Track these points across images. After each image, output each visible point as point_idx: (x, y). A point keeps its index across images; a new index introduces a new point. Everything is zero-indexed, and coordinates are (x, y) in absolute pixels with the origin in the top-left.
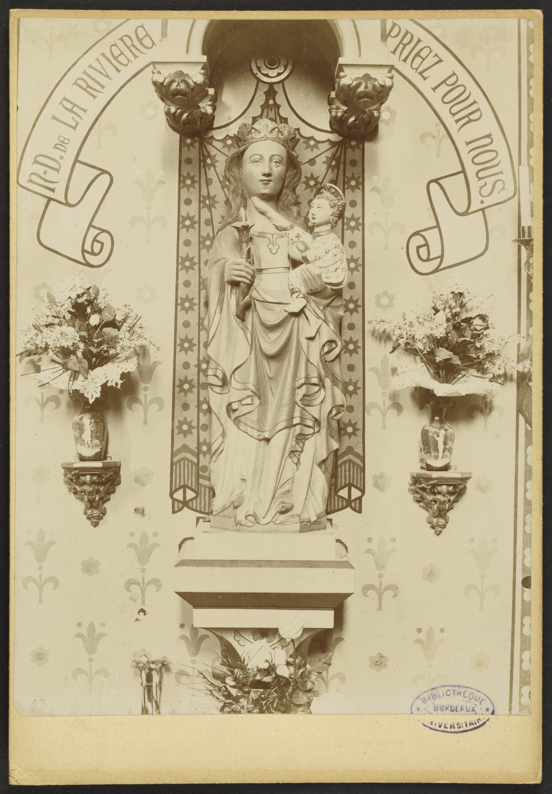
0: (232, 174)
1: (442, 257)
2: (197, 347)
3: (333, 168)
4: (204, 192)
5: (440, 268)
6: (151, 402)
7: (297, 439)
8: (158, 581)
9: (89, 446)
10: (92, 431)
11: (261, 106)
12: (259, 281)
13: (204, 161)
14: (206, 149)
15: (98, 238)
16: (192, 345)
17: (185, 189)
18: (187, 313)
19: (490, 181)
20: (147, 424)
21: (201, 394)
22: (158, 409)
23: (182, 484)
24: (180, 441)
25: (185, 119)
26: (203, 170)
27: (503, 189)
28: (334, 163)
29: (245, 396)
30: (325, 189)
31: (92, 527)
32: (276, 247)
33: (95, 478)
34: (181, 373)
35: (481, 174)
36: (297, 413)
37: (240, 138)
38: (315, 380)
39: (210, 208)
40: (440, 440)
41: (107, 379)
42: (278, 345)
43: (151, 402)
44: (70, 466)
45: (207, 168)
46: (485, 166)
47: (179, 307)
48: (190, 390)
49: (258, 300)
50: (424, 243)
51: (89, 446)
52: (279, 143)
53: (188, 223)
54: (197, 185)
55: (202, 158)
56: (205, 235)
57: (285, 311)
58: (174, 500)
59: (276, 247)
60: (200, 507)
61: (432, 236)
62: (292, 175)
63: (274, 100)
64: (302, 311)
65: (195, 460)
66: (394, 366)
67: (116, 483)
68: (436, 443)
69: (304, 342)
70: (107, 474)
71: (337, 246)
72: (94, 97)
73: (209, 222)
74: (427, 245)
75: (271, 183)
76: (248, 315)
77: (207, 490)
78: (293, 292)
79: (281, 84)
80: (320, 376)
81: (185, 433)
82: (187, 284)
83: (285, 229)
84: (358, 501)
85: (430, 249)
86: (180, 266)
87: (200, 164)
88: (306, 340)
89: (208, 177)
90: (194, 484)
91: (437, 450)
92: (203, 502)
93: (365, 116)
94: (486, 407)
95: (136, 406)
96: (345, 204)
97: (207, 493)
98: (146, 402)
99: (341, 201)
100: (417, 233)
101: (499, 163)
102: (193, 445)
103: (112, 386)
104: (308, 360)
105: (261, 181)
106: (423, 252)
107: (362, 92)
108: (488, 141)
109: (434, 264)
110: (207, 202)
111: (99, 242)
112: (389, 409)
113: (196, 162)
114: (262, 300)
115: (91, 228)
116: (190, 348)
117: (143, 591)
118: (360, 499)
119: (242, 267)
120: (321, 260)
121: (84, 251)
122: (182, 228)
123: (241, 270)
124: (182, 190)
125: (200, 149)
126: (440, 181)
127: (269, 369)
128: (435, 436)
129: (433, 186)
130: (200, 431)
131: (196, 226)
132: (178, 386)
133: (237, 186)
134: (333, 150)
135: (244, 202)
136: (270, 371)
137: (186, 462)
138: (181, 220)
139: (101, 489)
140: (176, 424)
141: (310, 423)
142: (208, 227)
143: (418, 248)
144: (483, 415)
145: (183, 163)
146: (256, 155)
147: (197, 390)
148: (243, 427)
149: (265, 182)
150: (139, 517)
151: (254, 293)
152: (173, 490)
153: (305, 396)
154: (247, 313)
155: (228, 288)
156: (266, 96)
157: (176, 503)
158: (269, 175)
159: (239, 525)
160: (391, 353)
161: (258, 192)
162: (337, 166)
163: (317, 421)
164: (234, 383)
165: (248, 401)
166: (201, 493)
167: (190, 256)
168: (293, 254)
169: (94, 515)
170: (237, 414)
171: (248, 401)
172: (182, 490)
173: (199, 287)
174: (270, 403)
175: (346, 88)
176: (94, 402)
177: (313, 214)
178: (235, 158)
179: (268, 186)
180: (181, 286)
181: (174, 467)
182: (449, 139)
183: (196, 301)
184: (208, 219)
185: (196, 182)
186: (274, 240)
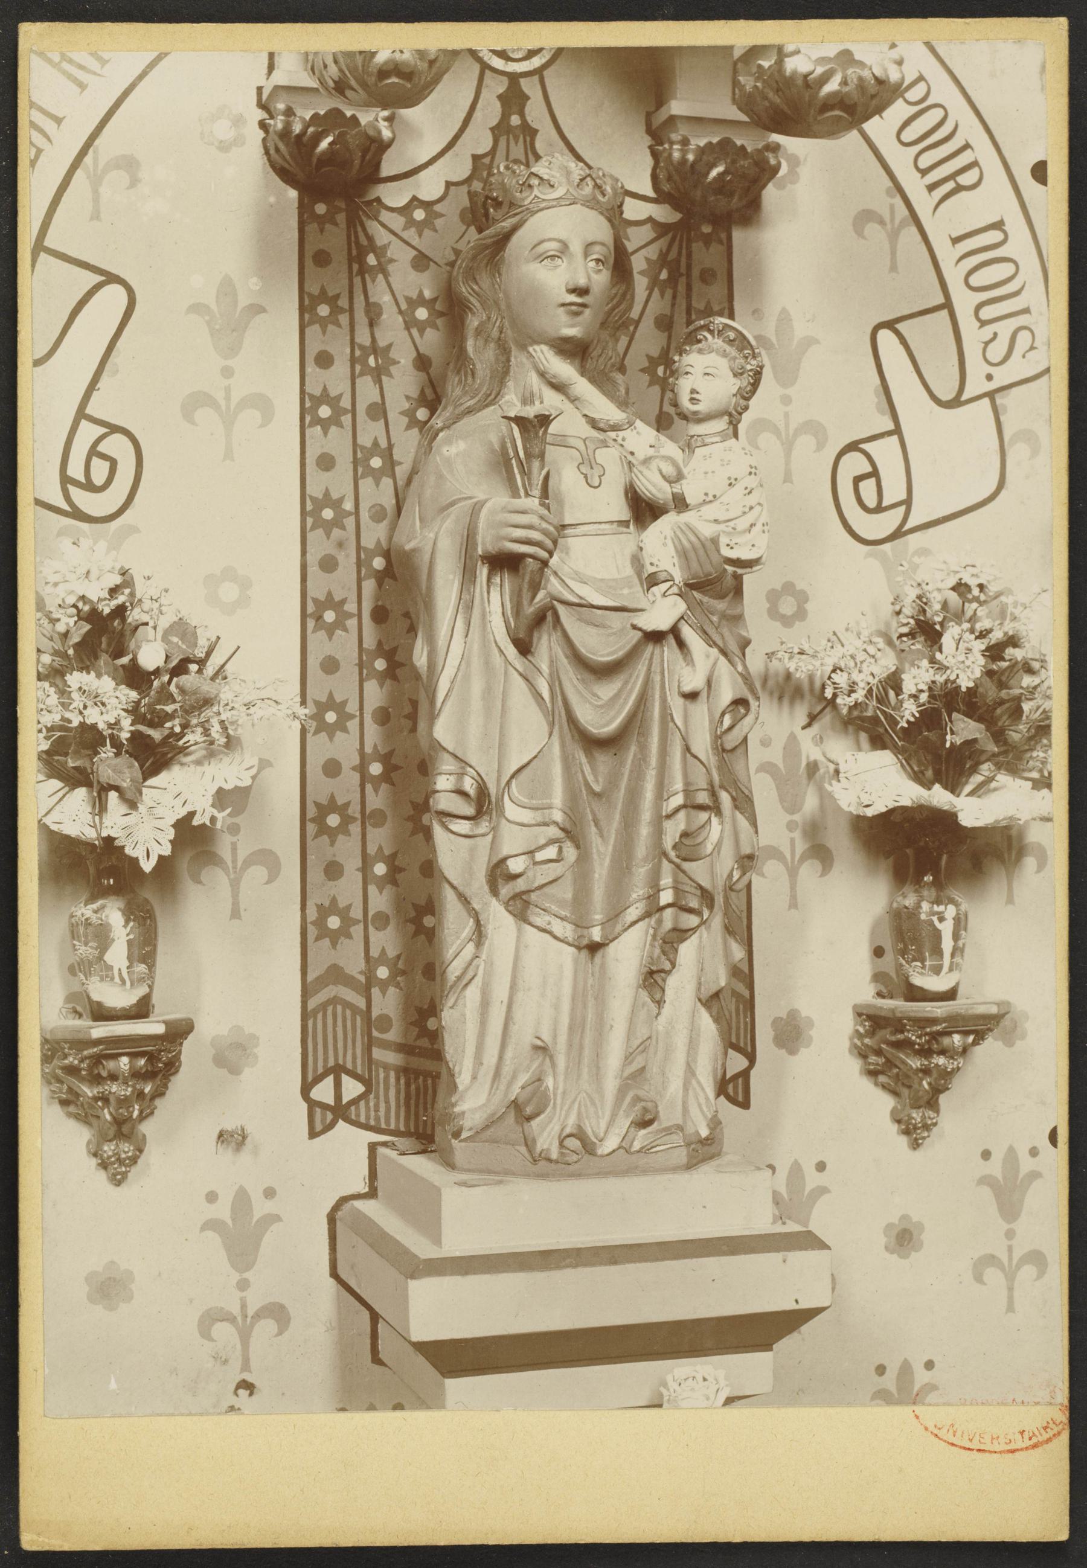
0: (475, 287)
1: (908, 502)
2: (357, 720)
3: (663, 286)
4: (363, 337)
5: (906, 528)
6: (248, 863)
7: (664, 942)
8: (282, 1307)
9: (123, 982)
10: (130, 943)
11: (492, 129)
12: (563, 555)
13: (360, 258)
14: (364, 229)
15: (101, 448)
16: (344, 717)
17: (316, 327)
18: (330, 635)
19: (1005, 329)
20: (240, 918)
21: (369, 837)
22: (266, 878)
23: (331, 1063)
24: (323, 955)
25: (324, 153)
26: (357, 280)
27: (1032, 348)
28: (664, 275)
29: (542, 841)
30: (711, 332)
31: (110, 1188)
32: (597, 471)
33: (142, 1062)
34: (321, 788)
35: (986, 313)
36: (666, 880)
37: (495, 199)
38: (703, 798)
39: (378, 375)
40: (946, 929)
41: (188, 808)
42: (619, 713)
43: (248, 863)
44: (81, 1036)
45: (367, 276)
46: (992, 295)
47: (311, 624)
48: (343, 828)
49: (563, 602)
50: (869, 469)
51: (123, 982)
52: (601, 213)
53: (325, 412)
54: (344, 319)
55: (354, 252)
56: (369, 444)
57: (634, 627)
58: (312, 1104)
59: (597, 471)
60: (377, 1119)
61: (886, 452)
62: (616, 294)
63: (522, 115)
64: (675, 631)
65: (361, 1003)
66: (812, 758)
67: (173, 1070)
68: (937, 935)
69: (677, 704)
70: (170, 1052)
71: (753, 470)
72: (82, 86)
73: (378, 411)
74: (875, 473)
75: (587, 312)
76: (539, 639)
77: (392, 1074)
78: (652, 581)
79: (536, 78)
80: (712, 786)
81: (334, 937)
82: (329, 564)
83: (615, 428)
84: (740, 1080)
85: (883, 484)
86: (310, 521)
87: (350, 268)
88: (681, 701)
89: (371, 300)
90: (359, 1062)
91: (938, 952)
92: (382, 1105)
93: (745, 163)
94: (1010, 847)
95: (207, 874)
96: (762, 367)
97: (392, 1080)
98: (234, 861)
99: (754, 362)
100: (853, 447)
101: (1023, 287)
102: (355, 966)
103: (204, 825)
104: (687, 749)
105: (563, 305)
106: (868, 488)
107: (835, 94)
108: (995, 236)
109: (889, 522)
110: (372, 361)
111: (104, 457)
112: (803, 859)
113: (339, 258)
114: (576, 600)
115: (84, 423)
116: (340, 726)
117: (245, 1337)
118: (745, 1074)
119: (534, 520)
120: (716, 504)
121: (66, 480)
122: (311, 425)
123: (530, 527)
124: (307, 330)
125: (348, 228)
126: (899, 326)
127: (595, 772)
128: (935, 919)
129: (884, 335)
130: (371, 928)
131: (347, 419)
132: (313, 820)
133: (489, 318)
134: (663, 243)
135: (504, 359)
136: (596, 777)
137: (339, 1008)
138: (308, 405)
139: (147, 1090)
140: (312, 914)
141: (694, 903)
142: (374, 424)
143: (858, 480)
144: (1003, 862)
145: (309, 262)
146: (550, 240)
147: (359, 829)
148: (540, 920)
149: (574, 308)
150: (227, 1154)
151: (554, 585)
152: (310, 1078)
153: (685, 835)
154: (536, 635)
155: (481, 573)
156: (503, 106)
157: (318, 1110)
158: (582, 292)
159: (543, 1163)
160: (804, 728)
161: (552, 333)
162: (673, 280)
163: (707, 897)
164: (511, 810)
165: (551, 852)
166: (378, 1083)
167: (335, 495)
168: (654, 491)
169: (123, 1156)
170: (520, 885)
171: (551, 852)
172: (330, 1080)
173: (359, 572)
174: (595, 856)
175: (800, 82)
176: (154, 869)
177: (693, 391)
178: (487, 247)
179: (580, 319)
180: (313, 570)
181: (310, 1023)
182: (914, 230)
183: (351, 607)
184: (376, 404)
185: (342, 310)
186: (590, 452)
